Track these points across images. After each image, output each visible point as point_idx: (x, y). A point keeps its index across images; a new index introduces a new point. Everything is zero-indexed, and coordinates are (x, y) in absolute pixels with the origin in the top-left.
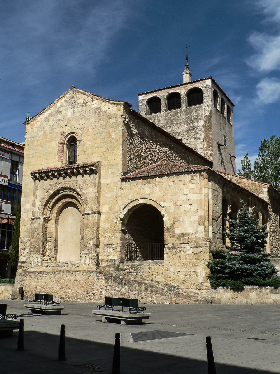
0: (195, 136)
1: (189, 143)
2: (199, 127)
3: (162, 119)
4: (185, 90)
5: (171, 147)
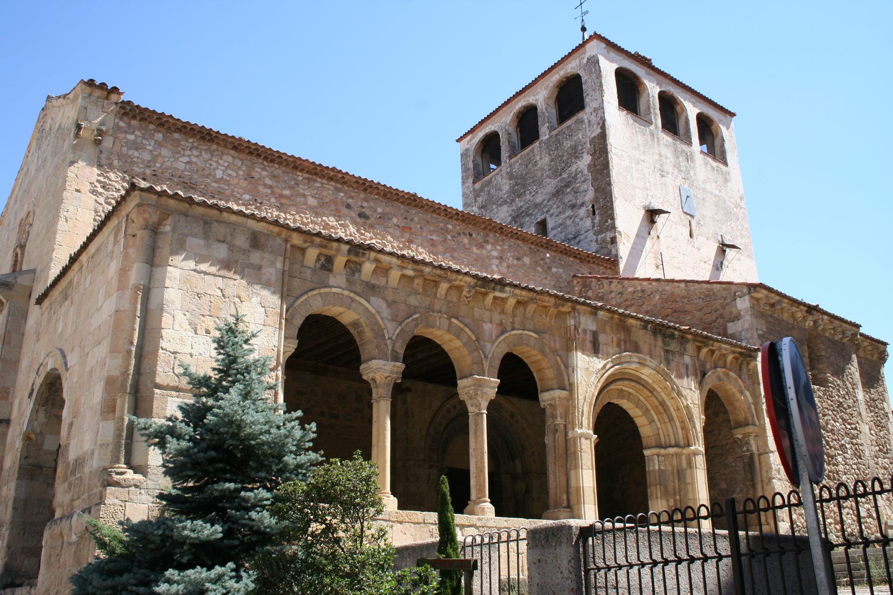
0: (574, 201)
1: (561, 224)
2: (580, 174)
3: (504, 181)
4: (545, 92)
5: (368, 212)
